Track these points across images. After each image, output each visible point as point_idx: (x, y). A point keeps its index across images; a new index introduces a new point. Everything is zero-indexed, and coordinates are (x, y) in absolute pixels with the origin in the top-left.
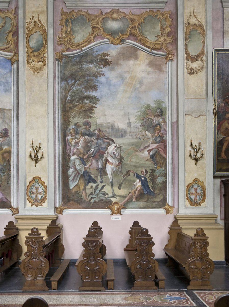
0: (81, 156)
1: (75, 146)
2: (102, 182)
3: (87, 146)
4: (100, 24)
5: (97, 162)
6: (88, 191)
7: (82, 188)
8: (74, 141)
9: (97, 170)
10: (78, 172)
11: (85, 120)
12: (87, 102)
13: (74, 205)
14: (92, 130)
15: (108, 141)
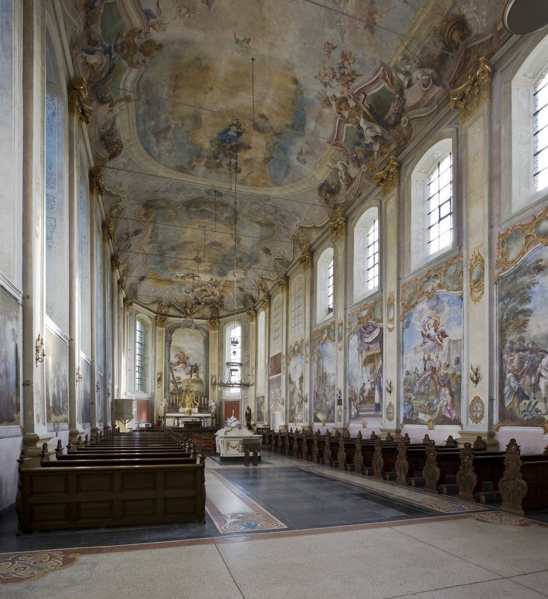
0: (515, 373)
1: (510, 364)
2: (535, 398)
3: (521, 362)
4: (533, 231)
5: (531, 377)
6: (522, 408)
7: (516, 405)
8: (509, 359)
9: (531, 386)
10: (512, 389)
11: (519, 336)
12: (521, 317)
13: (508, 423)
14: (525, 345)
15: (542, 353)
